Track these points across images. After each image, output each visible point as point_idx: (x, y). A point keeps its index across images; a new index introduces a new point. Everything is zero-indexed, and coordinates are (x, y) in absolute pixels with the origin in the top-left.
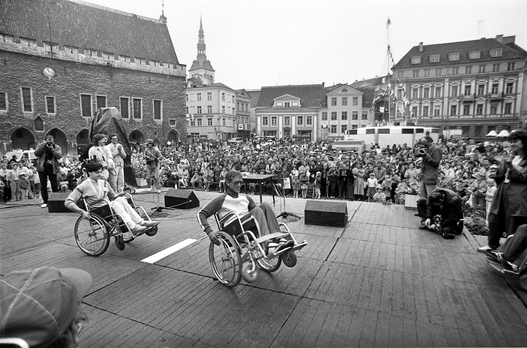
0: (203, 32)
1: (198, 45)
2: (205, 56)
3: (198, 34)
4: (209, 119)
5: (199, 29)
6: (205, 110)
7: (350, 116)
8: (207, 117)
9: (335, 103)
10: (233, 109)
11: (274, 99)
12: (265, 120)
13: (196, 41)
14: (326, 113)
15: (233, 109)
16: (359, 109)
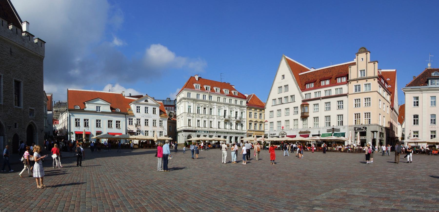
7: (150, 123)
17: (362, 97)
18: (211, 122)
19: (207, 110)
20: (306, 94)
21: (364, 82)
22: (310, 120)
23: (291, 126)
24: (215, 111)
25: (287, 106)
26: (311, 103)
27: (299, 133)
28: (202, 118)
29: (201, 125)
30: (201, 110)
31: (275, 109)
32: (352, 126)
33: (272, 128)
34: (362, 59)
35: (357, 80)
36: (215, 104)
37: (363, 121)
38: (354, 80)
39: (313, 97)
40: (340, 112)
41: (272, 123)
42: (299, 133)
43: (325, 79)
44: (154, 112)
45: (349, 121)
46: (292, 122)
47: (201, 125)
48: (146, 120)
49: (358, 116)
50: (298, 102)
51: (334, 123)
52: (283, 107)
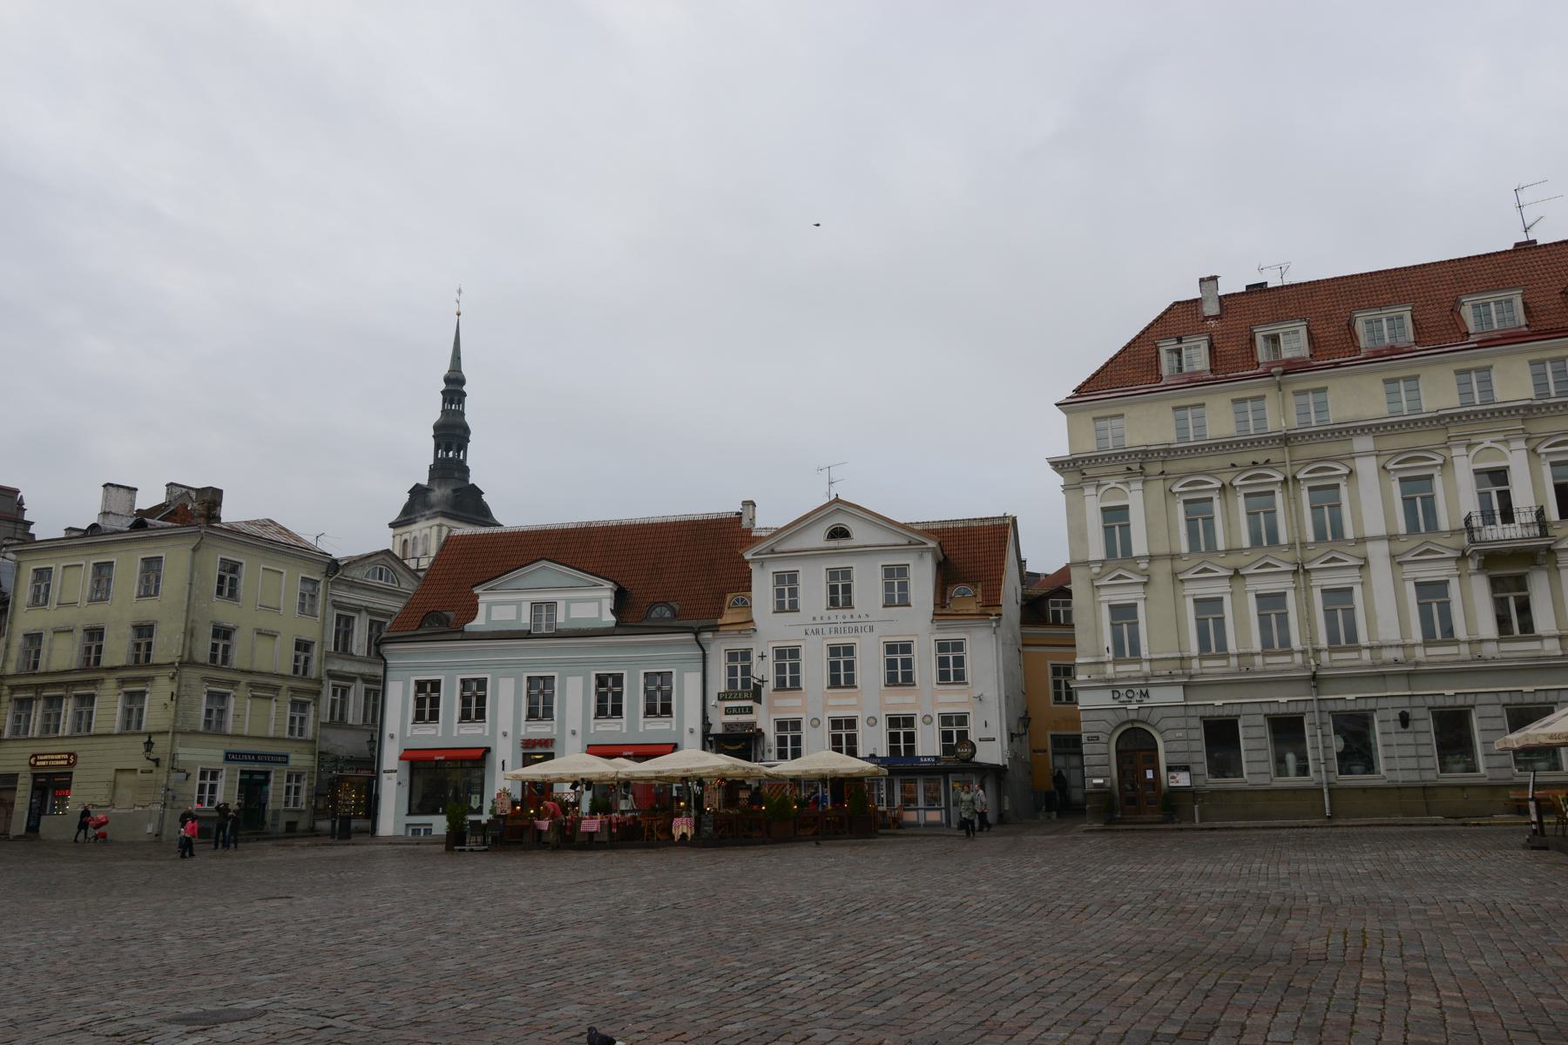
0: (462, 382)
1: (437, 427)
2: (466, 470)
3: (443, 386)
4: (131, 696)
5: (445, 368)
6: (117, 650)
7: (870, 665)
8: (123, 682)
9: (787, 601)
10: (303, 646)
11: (477, 591)
12: (427, 704)
13: (433, 410)
14: (746, 655)
15: (303, 646)
16: (916, 620)
24: (1371, 504)
28: (1237, 574)
29: (1243, 631)
30: (1232, 524)
36: (1363, 443)
44: (896, 591)
47: (1243, 631)
48: (834, 651)
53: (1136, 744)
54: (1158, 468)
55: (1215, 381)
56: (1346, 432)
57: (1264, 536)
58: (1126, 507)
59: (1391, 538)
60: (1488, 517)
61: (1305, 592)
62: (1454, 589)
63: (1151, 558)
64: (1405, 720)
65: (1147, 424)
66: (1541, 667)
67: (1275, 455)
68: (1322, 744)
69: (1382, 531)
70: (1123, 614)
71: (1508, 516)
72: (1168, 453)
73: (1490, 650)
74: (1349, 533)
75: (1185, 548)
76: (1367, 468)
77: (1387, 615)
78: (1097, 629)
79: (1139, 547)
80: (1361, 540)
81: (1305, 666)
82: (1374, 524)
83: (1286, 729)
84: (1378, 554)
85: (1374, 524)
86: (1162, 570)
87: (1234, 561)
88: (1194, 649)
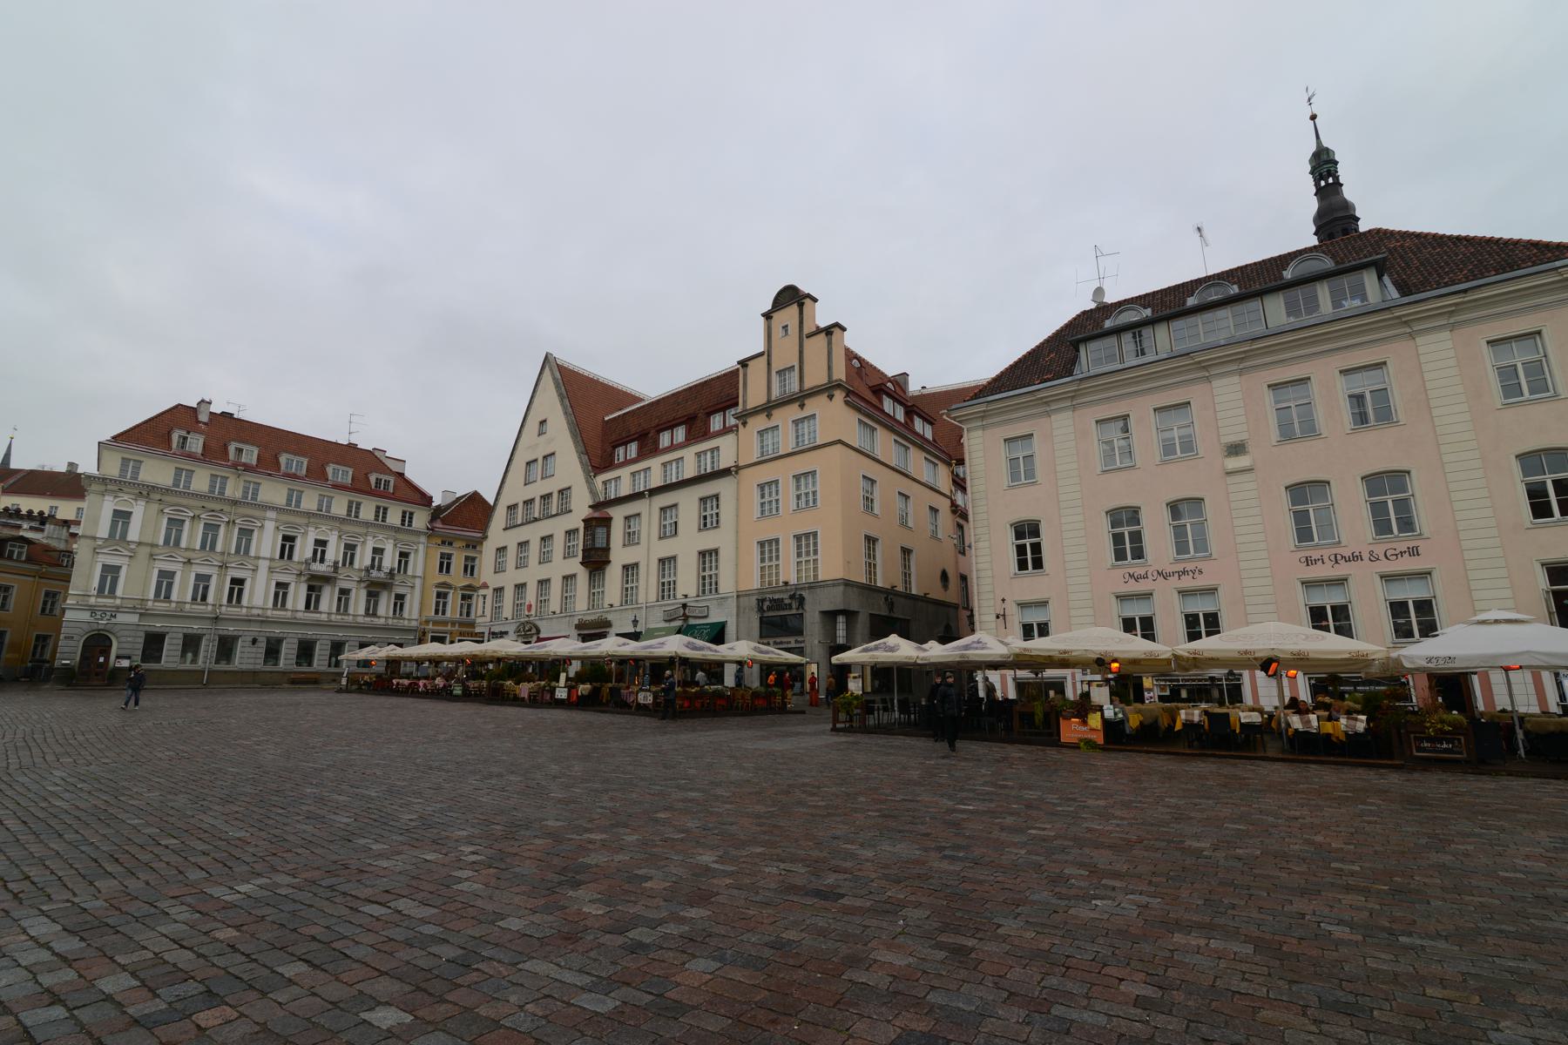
17: (782, 472)
18: (238, 582)
19: (226, 540)
20: (605, 483)
21: (793, 412)
22: (614, 573)
23: (555, 604)
25: (544, 528)
26: (618, 514)
27: (578, 627)
29: (182, 590)
30: (192, 535)
31: (511, 539)
32: (748, 594)
33: (497, 610)
34: (785, 327)
35: (768, 408)
36: (271, 514)
37: (789, 571)
38: (756, 411)
39: (625, 491)
40: (708, 540)
41: (499, 591)
42: (578, 627)
43: (671, 427)
45: (741, 574)
46: (556, 587)
47: (182, 590)
49: (768, 547)
50: (581, 507)
51: (687, 582)
52: (533, 533)
53: (98, 643)
54: (158, 497)
55: (204, 461)
56: (266, 507)
57: (208, 544)
58: (131, 513)
59: (272, 560)
60: (314, 560)
61: (221, 577)
62: (292, 588)
63: (140, 544)
64: (254, 641)
65: (157, 471)
66: (318, 625)
67: (227, 508)
68: (208, 649)
69: (268, 555)
70: (111, 572)
71: (322, 561)
72: (167, 491)
73: (300, 615)
74: (252, 553)
75: (161, 542)
76: (270, 526)
77: (258, 594)
78: (90, 577)
79: (133, 534)
80: (258, 558)
81: (214, 611)
82: (266, 553)
83: (191, 643)
84: (264, 566)
85: (266, 553)
86: (144, 551)
87: (189, 554)
88: (152, 596)
